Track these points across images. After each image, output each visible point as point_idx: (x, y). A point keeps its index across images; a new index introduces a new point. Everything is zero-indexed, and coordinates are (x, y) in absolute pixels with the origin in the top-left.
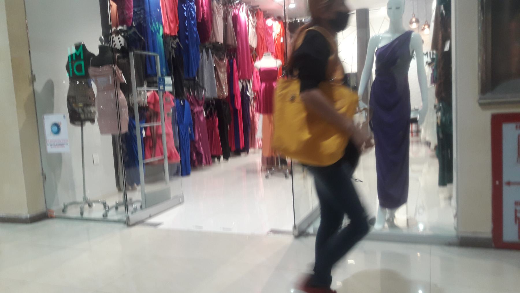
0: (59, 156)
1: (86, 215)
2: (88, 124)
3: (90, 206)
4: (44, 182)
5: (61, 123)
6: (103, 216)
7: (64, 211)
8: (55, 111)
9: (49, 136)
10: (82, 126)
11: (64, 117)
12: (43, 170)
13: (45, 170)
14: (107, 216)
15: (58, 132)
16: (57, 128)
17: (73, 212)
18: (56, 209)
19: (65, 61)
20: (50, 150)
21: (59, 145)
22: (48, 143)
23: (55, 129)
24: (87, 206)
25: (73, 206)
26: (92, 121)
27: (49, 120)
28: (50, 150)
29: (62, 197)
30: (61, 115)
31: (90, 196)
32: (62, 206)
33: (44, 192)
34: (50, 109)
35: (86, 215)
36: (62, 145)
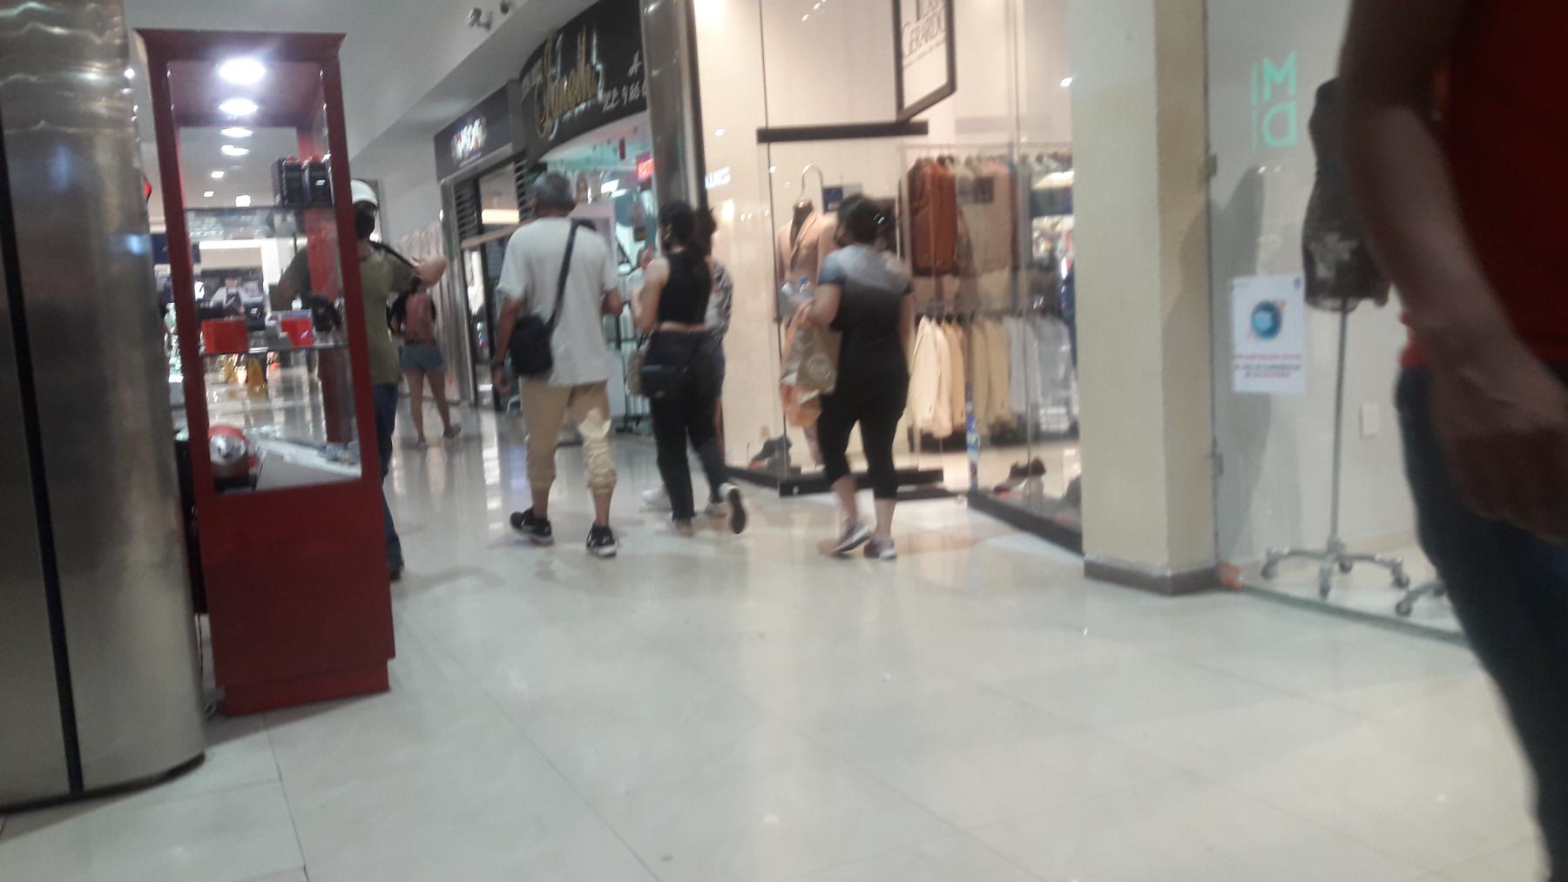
0: (1260, 405)
1: (1334, 597)
2: (1366, 306)
3: (1345, 569)
4: (1215, 477)
5: (1283, 303)
6: (1398, 607)
7: (1266, 573)
8: (1259, 269)
9: (1244, 342)
10: (1344, 310)
11: (1297, 282)
12: (1215, 443)
13: (1221, 441)
14: (1408, 612)
15: (1272, 331)
16: (1271, 318)
17: (1296, 580)
18: (1244, 561)
19: (1298, 110)
20: (1243, 383)
21: (1273, 367)
22: (1241, 362)
23: (1265, 320)
24: (1336, 567)
25: (1293, 561)
26: (1381, 299)
27: (1246, 295)
28: (1243, 383)
29: (1264, 532)
30: (1275, 276)
31: (1353, 538)
32: (1261, 557)
33: (1215, 507)
34: (1245, 263)
35: (1334, 597)
36: (1282, 370)
